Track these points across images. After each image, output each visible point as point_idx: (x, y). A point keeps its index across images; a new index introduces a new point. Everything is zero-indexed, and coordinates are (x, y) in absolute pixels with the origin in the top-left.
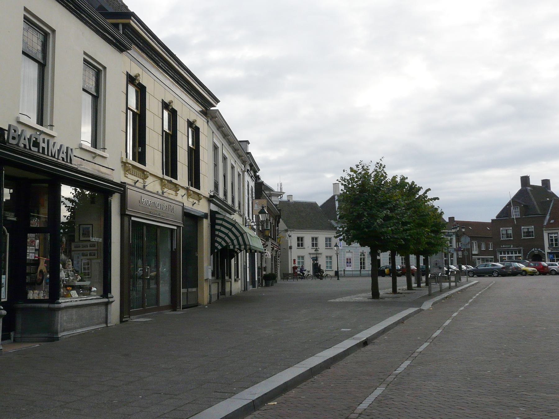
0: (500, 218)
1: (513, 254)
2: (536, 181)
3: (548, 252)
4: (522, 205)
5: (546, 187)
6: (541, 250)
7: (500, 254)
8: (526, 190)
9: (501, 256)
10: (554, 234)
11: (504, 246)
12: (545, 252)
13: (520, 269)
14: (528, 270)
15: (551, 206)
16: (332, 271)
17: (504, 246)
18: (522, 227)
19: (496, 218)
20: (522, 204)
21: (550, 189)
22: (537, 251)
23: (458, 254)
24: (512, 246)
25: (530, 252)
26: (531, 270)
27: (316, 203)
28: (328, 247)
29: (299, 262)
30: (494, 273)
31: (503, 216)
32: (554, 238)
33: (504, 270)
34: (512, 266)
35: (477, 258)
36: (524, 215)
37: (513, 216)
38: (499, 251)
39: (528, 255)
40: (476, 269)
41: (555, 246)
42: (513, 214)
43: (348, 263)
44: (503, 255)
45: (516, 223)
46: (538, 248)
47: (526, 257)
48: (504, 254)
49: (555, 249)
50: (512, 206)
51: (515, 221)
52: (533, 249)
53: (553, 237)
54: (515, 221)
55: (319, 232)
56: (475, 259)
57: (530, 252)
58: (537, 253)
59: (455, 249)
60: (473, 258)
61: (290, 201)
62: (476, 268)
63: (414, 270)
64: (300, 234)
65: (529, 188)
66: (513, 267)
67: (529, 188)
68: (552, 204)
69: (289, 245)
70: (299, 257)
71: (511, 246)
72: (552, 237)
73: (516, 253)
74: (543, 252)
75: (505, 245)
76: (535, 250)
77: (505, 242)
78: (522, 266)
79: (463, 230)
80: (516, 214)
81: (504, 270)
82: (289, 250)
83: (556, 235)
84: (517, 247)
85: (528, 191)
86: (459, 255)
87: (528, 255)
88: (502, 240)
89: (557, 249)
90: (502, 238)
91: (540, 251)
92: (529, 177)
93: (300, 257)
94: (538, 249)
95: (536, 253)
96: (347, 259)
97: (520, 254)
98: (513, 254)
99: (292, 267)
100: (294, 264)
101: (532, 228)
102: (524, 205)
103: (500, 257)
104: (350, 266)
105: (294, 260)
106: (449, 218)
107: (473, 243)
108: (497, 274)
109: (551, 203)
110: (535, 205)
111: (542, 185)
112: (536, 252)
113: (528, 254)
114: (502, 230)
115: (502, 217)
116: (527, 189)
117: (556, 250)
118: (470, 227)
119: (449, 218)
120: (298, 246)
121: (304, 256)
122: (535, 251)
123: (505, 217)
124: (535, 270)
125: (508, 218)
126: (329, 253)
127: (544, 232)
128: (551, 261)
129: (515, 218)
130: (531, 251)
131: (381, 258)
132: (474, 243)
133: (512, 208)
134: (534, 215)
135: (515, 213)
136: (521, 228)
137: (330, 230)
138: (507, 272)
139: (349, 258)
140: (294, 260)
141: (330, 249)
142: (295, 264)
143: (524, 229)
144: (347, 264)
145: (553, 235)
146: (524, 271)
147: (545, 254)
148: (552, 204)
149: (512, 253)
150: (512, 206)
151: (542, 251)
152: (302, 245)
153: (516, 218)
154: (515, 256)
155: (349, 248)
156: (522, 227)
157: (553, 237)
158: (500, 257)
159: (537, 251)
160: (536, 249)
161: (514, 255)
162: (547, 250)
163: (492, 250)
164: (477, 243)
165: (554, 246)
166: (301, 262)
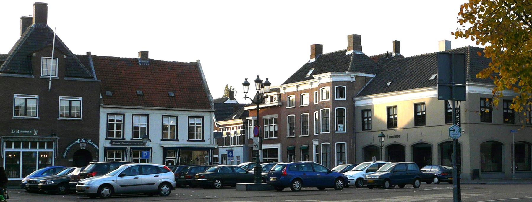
1: (36, 148)
4: (65, 57)
7: (6, 147)
9: (42, 150)
10: (116, 116)
11: (18, 131)
12: (98, 146)
17: (18, 131)
22: (85, 145)
24: (36, 133)
31: (17, 71)
32: (115, 122)
39: (66, 152)
41: (116, 137)
45: (50, 89)
47: (63, 154)
49: (117, 142)
52: (77, 140)
57: (71, 146)
58: (85, 148)
71: (33, 132)
72: (113, 121)
74: (96, 146)
75: (20, 130)
83: (120, 118)
87: (66, 152)
88: (15, 119)
89: (121, 142)
95: (81, 148)
98: (36, 148)
101: (77, 103)
112: (83, 146)
113: (68, 149)
115: (15, 73)
122: (81, 145)
125: (33, 77)
127: (101, 110)
128: (231, 164)
129: (50, 79)
130: (74, 143)
143: (63, 102)
145: (116, 118)
147: (98, 151)
151: (94, 145)
158: (6, 152)
159: (85, 145)
162: (104, 143)
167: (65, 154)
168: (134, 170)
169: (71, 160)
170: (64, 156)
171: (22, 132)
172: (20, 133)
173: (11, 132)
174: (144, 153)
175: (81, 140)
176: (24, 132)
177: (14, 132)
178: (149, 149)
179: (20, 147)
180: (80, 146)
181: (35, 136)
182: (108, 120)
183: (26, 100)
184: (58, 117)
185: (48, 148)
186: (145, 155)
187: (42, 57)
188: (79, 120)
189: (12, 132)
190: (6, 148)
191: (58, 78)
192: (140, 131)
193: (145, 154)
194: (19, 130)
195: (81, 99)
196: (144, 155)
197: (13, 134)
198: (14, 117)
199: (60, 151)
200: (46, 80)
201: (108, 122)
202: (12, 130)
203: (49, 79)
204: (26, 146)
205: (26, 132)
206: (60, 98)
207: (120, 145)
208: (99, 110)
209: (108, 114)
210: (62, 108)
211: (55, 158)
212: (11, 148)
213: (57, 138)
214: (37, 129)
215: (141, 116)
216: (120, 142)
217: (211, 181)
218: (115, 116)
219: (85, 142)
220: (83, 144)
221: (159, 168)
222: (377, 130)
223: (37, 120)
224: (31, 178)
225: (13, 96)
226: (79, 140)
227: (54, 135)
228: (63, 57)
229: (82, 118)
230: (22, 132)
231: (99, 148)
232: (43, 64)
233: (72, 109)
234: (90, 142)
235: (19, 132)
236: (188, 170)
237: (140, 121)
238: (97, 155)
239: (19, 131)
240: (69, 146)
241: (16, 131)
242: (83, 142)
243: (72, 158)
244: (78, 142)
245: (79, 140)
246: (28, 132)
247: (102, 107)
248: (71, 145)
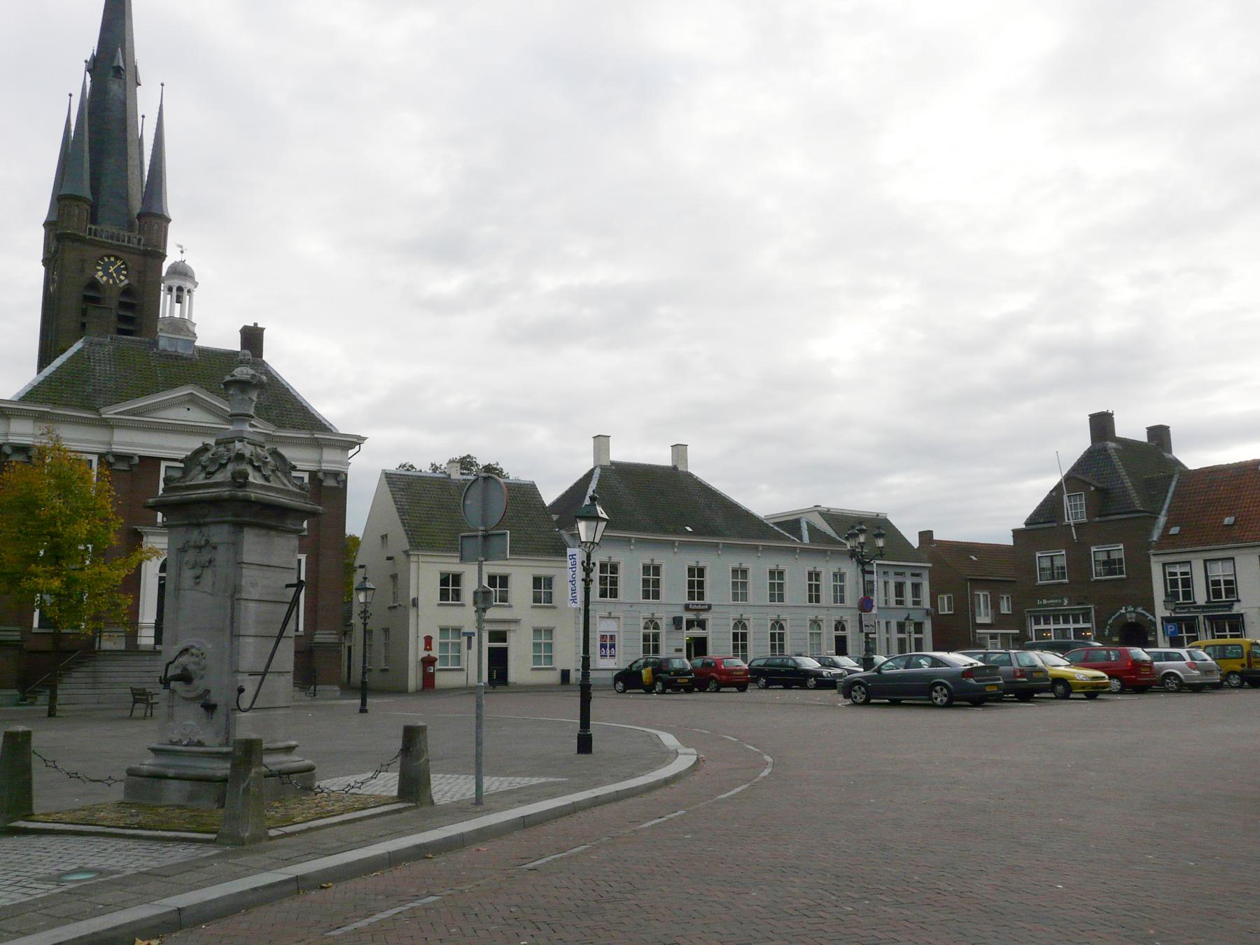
0: (1034, 527)
2: (1130, 427)
3: (1162, 618)
5: (1158, 444)
6: (1143, 612)
7: (1035, 624)
8: (1105, 449)
10: (1180, 566)
11: (1045, 602)
12: (1155, 617)
13: (1041, 675)
14: (1075, 678)
15: (1172, 489)
16: (551, 672)
17: (1045, 602)
18: (1093, 549)
19: (1024, 526)
20: (1093, 486)
21: (1170, 451)
22: (1134, 615)
23: (861, 622)
24: (1066, 602)
25: (1113, 617)
26: (1086, 676)
27: (535, 485)
28: (542, 604)
29: (443, 646)
30: (936, 692)
31: (1042, 521)
32: (1179, 576)
33: (972, 681)
34: (1012, 665)
35: (990, 633)
36: (1100, 516)
37: (1069, 519)
38: (1032, 614)
39: (1108, 627)
40: (876, 673)
41: (1183, 599)
42: (1068, 513)
43: (605, 649)
44: (1042, 627)
45: (1075, 538)
48: (1045, 624)
49: (1183, 608)
50: (1065, 492)
51: (1074, 531)
52: (1122, 609)
53: (1179, 574)
54: (1074, 531)
55: (536, 562)
56: (985, 636)
57: (1113, 617)
58: (1134, 621)
59: (927, 610)
60: (979, 633)
61: (452, 477)
62: (874, 671)
63: (737, 670)
64: (452, 565)
65: (1111, 445)
66: (1018, 667)
67: (1111, 445)
68: (1174, 484)
69: (412, 595)
70: (444, 630)
71: (1063, 602)
72: (1175, 574)
73: (1076, 621)
74: (1151, 617)
76: (1126, 612)
77: (1047, 591)
78: (1056, 664)
79: (880, 543)
80: (1077, 513)
81: (972, 681)
82: (412, 612)
83: (1186, 569)
84: (1078, 604)
85: (1110, 451)
86: (864, 623)
87: (1108, 627)
88: (1039, 586)
89: (1189, 608)
90: (1041, 580)
91: (1141, 613)
92: (1113, 414)
93: (448, 630)
95: (1129, 621)
96: (603, 637)
99: (420, 658)
100: (426, 649)
102: (1097, 489)
103: (1035, 630)
104: (612, 656)
105: (428, 640)
106: (920, 533)
107: (979, 595)
108: (945, 696)
109: (1171, 481)
110: (1126, 487)
111: (1148, 440)
112: (1131, 618)
113: (1109, 622)
114: (1039, 557)
115: (1040, 523)
116: (1105, 448)
117: (1186, 610)
118: (973, 557)
119: (920, 533)
120: (537, 599)
121: (554, 628)
122: (1128, 615)
123: (1049, 522)
124: (1103, 678)
125: (1055, 525)
126: (543, 618)
127: (1153, 559)
129: (1072, 524)
131: (710, 634)
132: (981, 596)
133: (1065, 497)
134: (1126, 513)
135: (1074, 512)
136: (1090, 550)
137: (549, 554)
138: (982, 689)
139: (608, 634)
140: (428, 640)
141: (547, 607)
142: (431, 649)
143: (1098, 552)
144: (601, 651)
145: (1178, 569)
146: (1061, 680)
147: (1155, 624)
148: (1174, 484)
149: (1066, 621)
150: (1065, 492)
151: (1148, 614)
152: (549, 598)
153: (1075, 524)
154: (1074, 629)
155: (610, 608)
156: (1093, 549)
157: (1179, 574)
158: (1035, 630)
159: (1134, 615)
160: (1129, 609)
161: (1072, 626)
162: (1161, 611)
163: (1010, 612)
164: (989, 596)
165: (1181, 601)
166: (450, 644)
167: (1107, 630)
168: (1161, 656)
169: (1116, 639)
171: (1049, 602)
174: (1169, 626)
176: (1052, 601)
178: (1240, 616)
182: (1167, 573)
184: (1092, 577)
185: (1045, 624)
186: (1172, 630)
190: (1035, 624)
192: (1223, 587)
193: (1171, 628)
196: (1169, 630)
197: (1039, 606)
198: (1039, 582)
199: (1100, 625)
201: (1168, 577)
203: (1070, 525)
204: (1056, 621)
207: (1189, 612)
208: (1149, 561)
209: (1164, 565)
212: (1079, 623)
216: (1187, 607)
217: (1023, 678)
218: (1178, 566)
219: (1133, 612)
221: (1171, 654)
222: (262, 638)
224: (1080, 664)
226: (1124, 608)
228: (1090, 488)
230: (1049, 602)
234: (1141, 611)
237: (1220, 571)
244: (1123, 611)
245: (1124, 608)
246: (1057, 601)
247: (1154, 555)
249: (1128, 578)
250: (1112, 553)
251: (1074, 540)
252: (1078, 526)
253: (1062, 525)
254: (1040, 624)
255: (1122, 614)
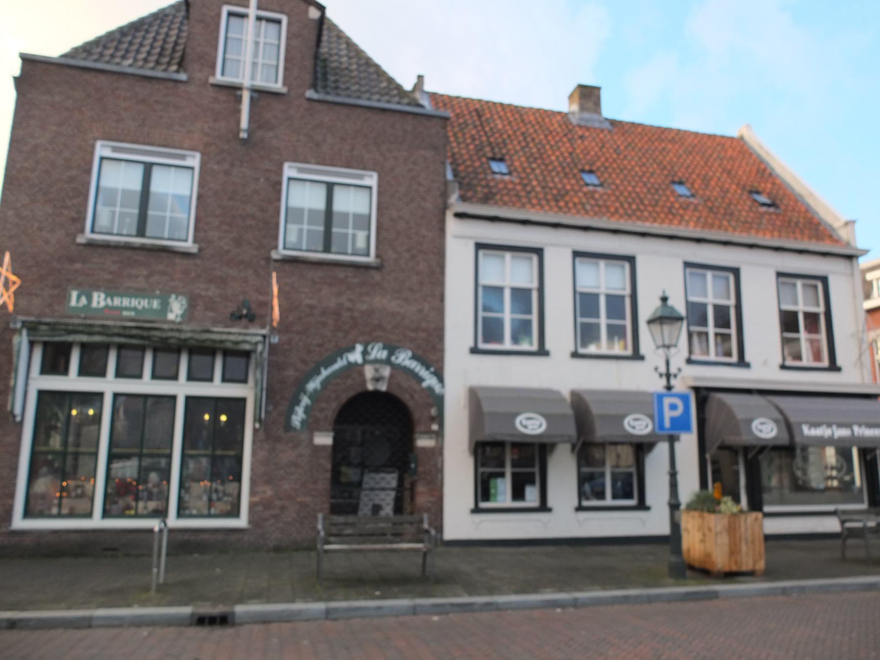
6: (414, 365)
11: (99, 300)
12: (441, 379)
17: (99, 300)
22: (386, 372)
24: (176, 309)
25: (325, 373)
39: (305, 400)
46: (392, 350)
47: (291, 411)
48: (83, 371)
52: (352, 349)
57: (325, 373)
58: (383, 387)
71: (165, 306)
75: (110, 294)
76: (365, 362)
84: (237, 317)
94: (391, 353)
95: (370, 387)
97: (245, 381)
114: (102, 159)
122: (369, 372)
130: (340, 364)
147: (439, 401)
151: (423, 373)
170: (298, 417)
172: (107, 307)
173: (69, 301)
175: (369, 348)
177: (84, 301)
179: (102, 373)
180: (362, 374)
181: (173, 322)
183: (148, 169)
184: (276, 247)
187: (225, 9)
188: (366, 267)
189: (73, 302)
191: (284, 90)
194: (103, 296)
195: (372, 180)
200: (234, 90)
202: (74, 294)
205: (134, 302)
206: (289, 170)
210: (295, 215)
211: (257, 425)
213: (264, 336)
214: (182, 294)
215: (606, 265)
219: (388, 362)
220: (377, 370)
223: (186, 255)
225: (93, 147)
226: (359, 348)
227: (246, 316)
229: (378, 256)
230: (117, 301)
231: (443, 386)
232: (226, 38)
233: (335, 220)
235: (102, 304)
236: (861, 490)
238: (432, 419)
239: (105, 299)
240: (318, 373)
241: (90, 299)
242: (376, 361)
243: (327, 430)
244: (356, 356)
245: (359, 348)
248: (326, 368)
249: (378, 268)
250: (338, 193)
251: (238, 129)
252: (260, 95)
253: (205, 83)
254: (65, 371)
255: (351, 366)
